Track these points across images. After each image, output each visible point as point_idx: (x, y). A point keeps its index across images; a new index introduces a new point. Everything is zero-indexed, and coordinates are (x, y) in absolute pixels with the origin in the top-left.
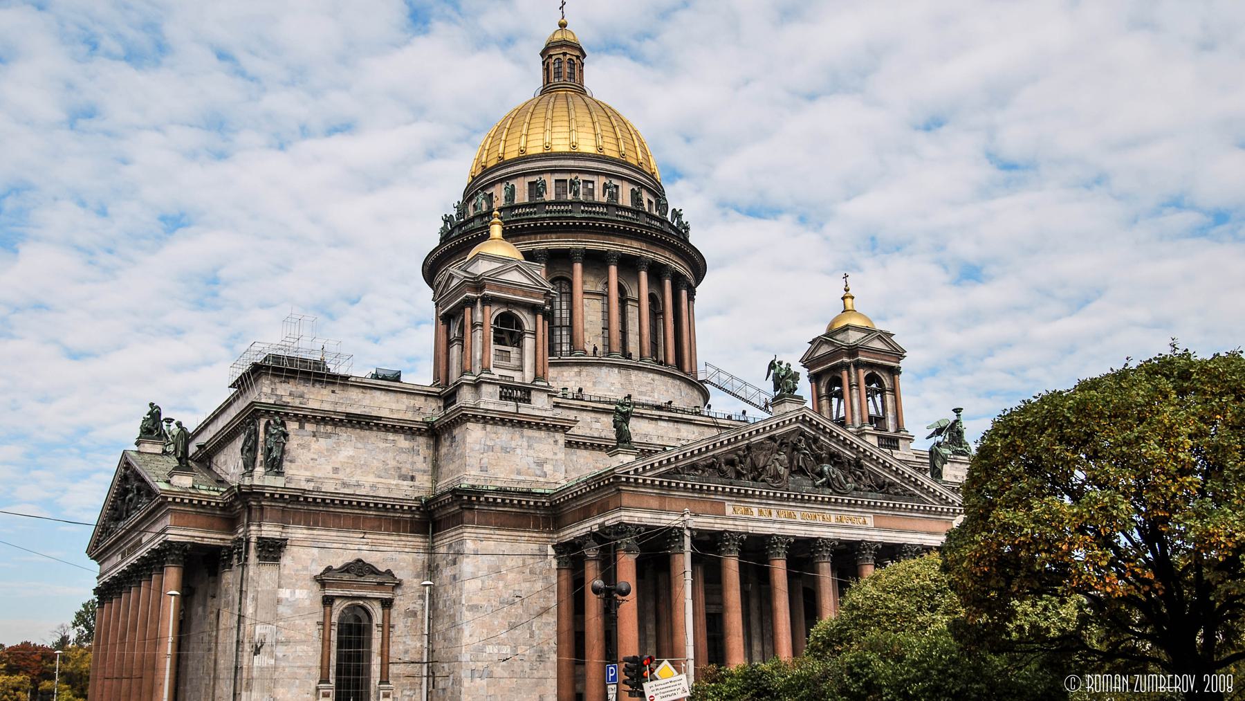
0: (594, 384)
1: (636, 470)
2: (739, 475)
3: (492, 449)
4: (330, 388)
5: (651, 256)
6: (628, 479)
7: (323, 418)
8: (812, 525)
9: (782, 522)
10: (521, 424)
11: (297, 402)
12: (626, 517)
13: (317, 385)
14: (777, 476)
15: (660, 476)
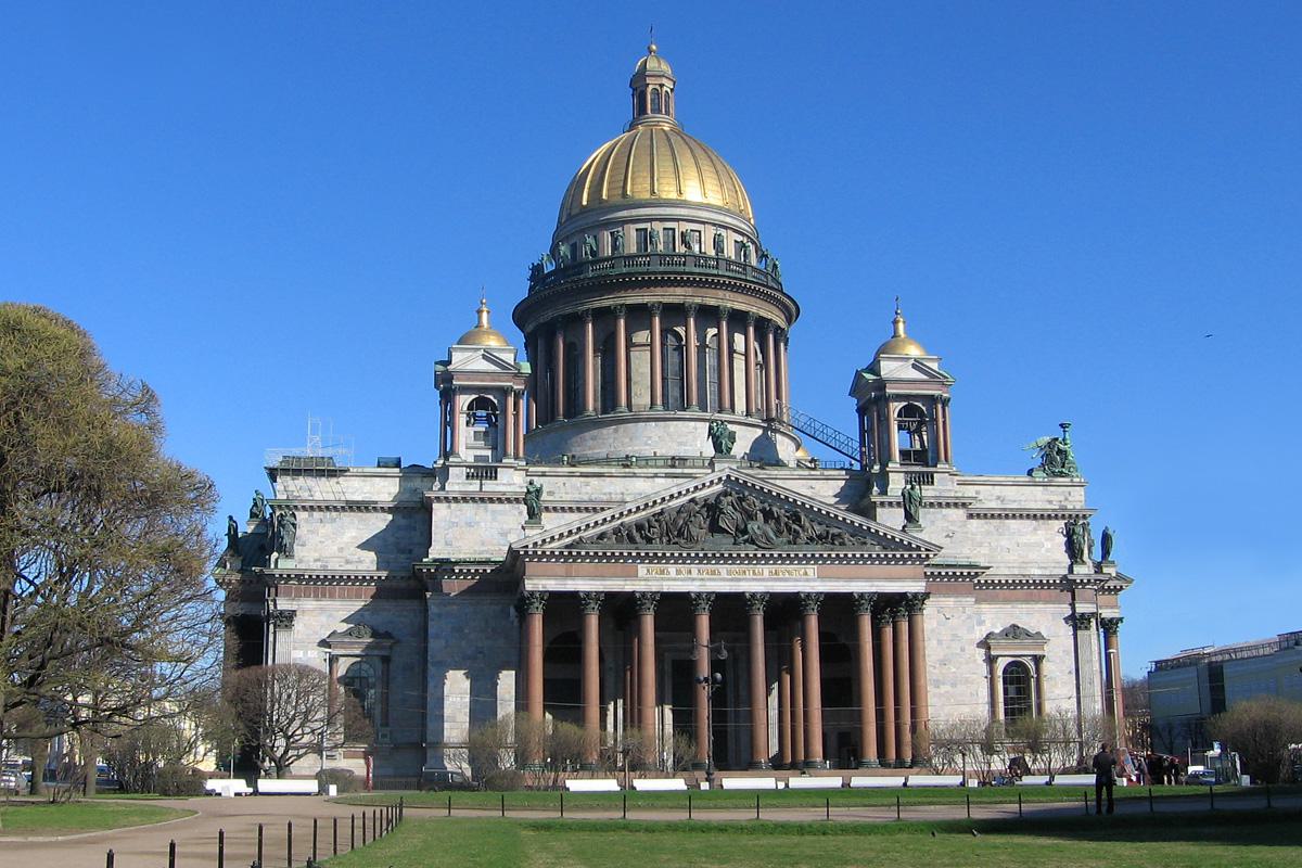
0: (631, 439)
1: (535, 544)
2: (649, 540)
3: (456, 524)
4: (334, 480)
5: (698, 300)
6: (526, 552)
7: (327, 508)
8: (739, 580)
9: (702, 579)
10: (482, 500)
11: (305, 495)
12: (529, 585)
13: (323, 479)
14: (690, 538)
15: (567, 547)
